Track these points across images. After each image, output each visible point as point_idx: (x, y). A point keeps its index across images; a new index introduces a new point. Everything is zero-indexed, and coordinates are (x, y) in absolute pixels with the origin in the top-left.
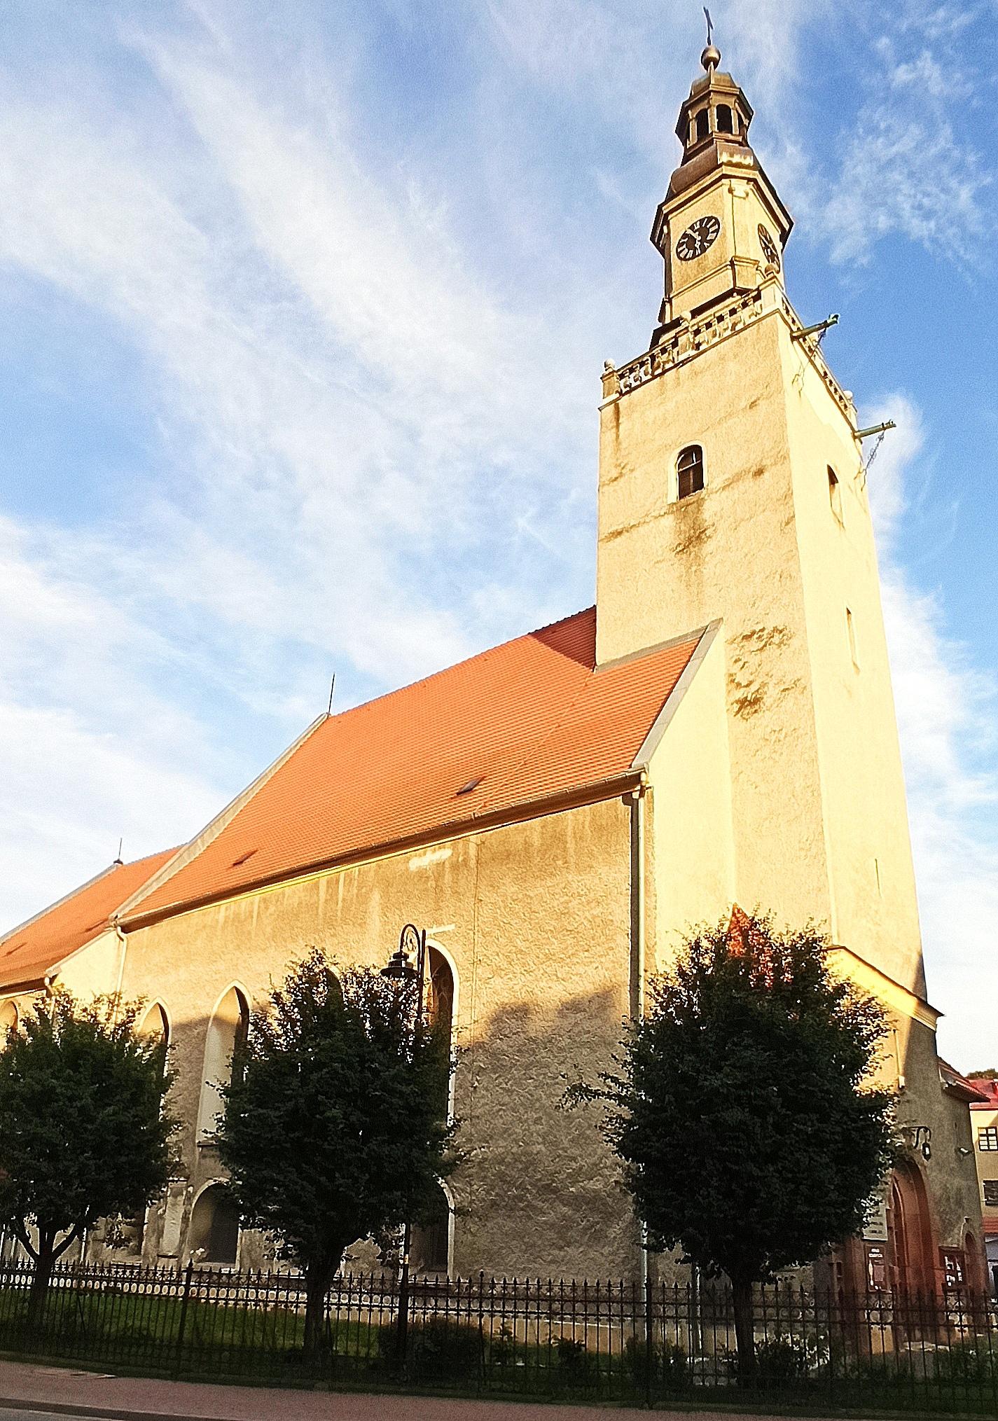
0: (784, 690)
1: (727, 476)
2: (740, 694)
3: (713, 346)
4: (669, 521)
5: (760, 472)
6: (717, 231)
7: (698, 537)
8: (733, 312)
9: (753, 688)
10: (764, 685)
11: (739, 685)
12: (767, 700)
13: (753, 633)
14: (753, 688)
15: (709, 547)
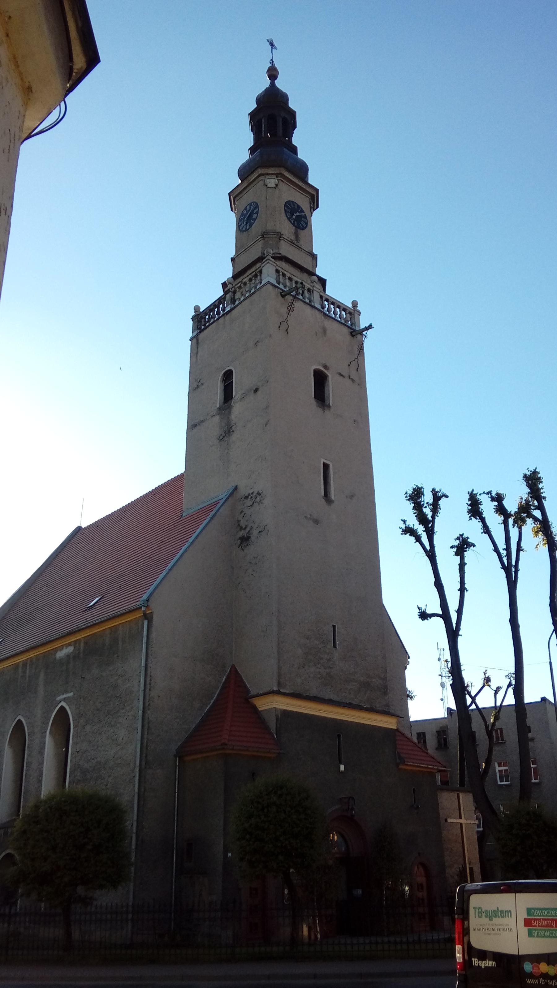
0: (259, 532)
1: (243, 391)
2: (241, 533)
3: (254, 293)
4: (217, 418)
5: (256, 390)
6: (257, 213)
7: (229, 432)
8: (250, 280)
9: (248, 529)
10: (252, 528)
11: (241, 528)
12: (253, 538)
13: (249, 495)
14: (248, 529)
15: (234, 437)
